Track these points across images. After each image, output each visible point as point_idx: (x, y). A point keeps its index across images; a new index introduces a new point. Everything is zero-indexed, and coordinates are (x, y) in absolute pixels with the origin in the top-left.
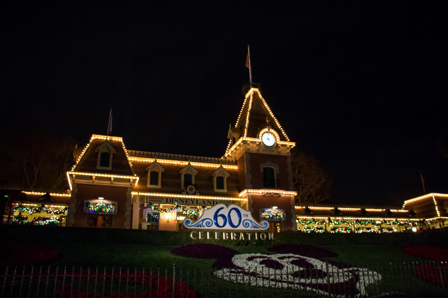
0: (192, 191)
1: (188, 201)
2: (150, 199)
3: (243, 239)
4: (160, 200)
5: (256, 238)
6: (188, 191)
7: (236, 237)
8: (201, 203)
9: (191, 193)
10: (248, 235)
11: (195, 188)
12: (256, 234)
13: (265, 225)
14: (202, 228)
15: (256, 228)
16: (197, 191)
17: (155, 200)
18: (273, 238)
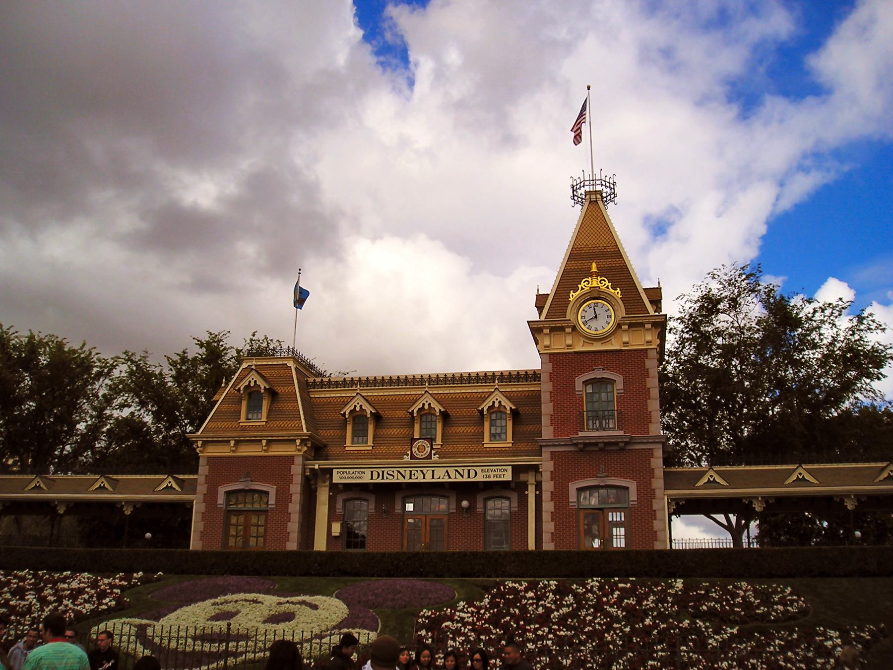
1: (414, 475)
8: (441, 477)
9: (422, 455)
11: (429, 445)
16: (433, 452)
17: (349, 475)
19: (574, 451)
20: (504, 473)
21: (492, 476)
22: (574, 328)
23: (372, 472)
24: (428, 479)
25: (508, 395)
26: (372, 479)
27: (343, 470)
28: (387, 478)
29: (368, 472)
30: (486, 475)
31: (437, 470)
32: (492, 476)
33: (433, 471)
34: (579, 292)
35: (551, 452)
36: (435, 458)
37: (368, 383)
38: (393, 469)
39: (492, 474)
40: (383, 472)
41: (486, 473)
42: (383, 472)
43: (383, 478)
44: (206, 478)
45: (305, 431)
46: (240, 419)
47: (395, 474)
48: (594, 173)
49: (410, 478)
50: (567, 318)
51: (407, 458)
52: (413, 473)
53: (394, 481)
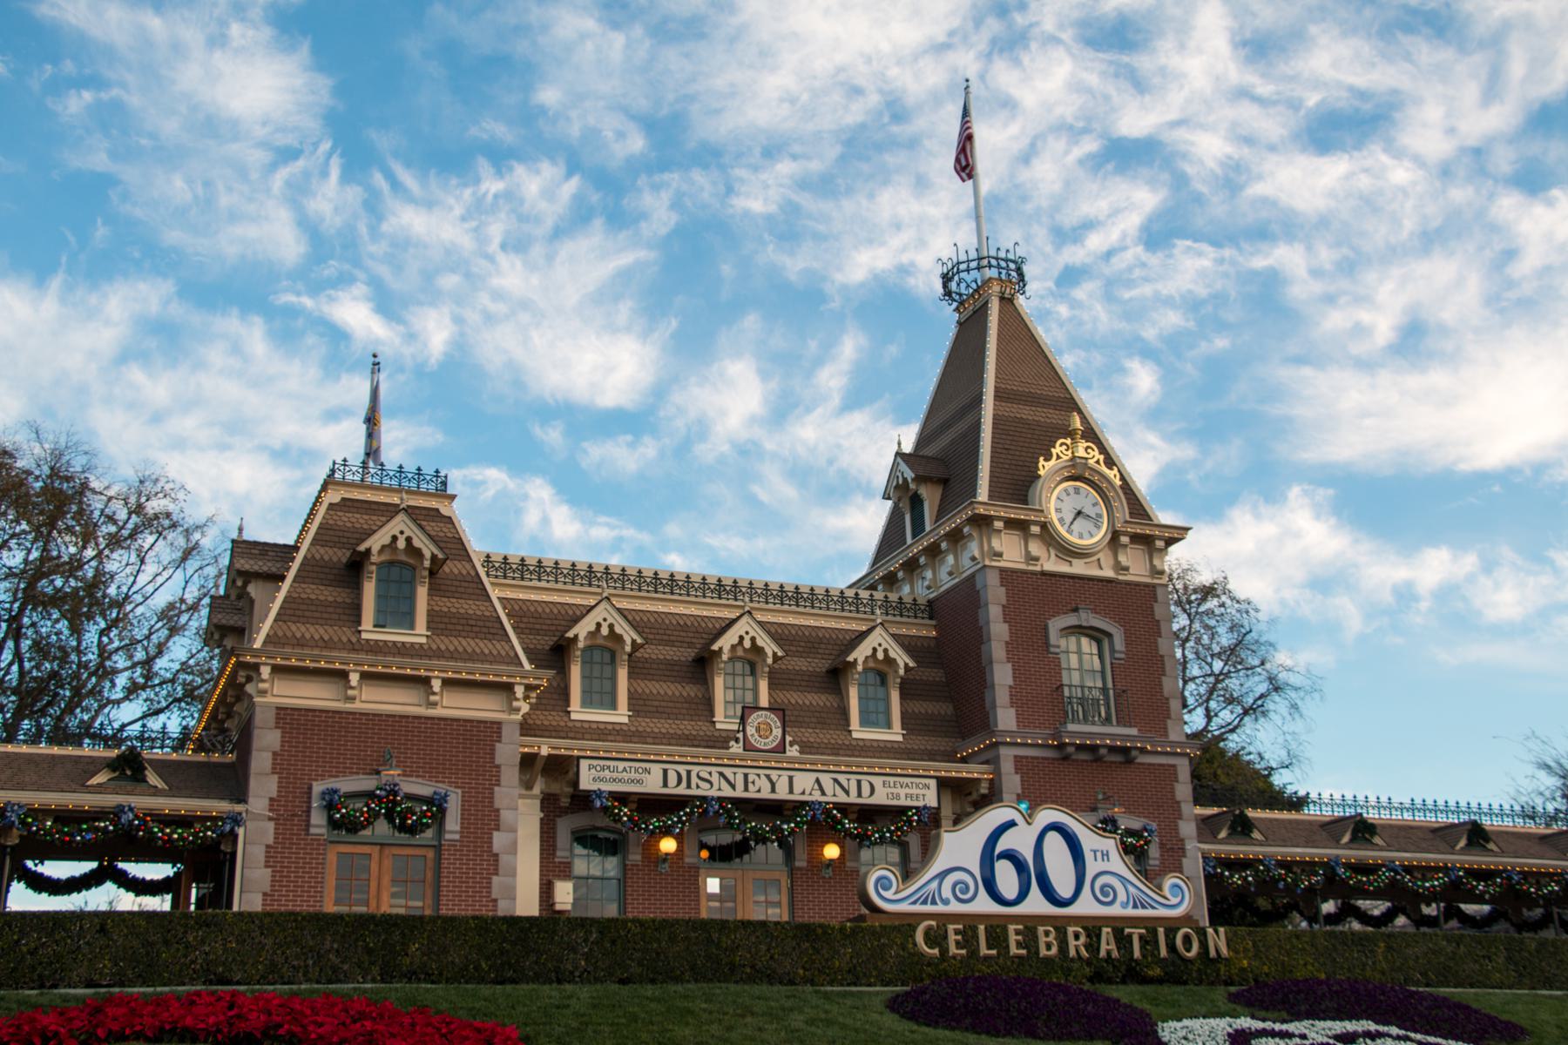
0: (767, 738)
1: (753, 783)
2: (593, 771)
3: (1115, 954)
4: (637, 776)
5: (1163, 952)
6: (752, 735)
7: (1087, 946)
8: (807, 792)
9: (765, 744)
10: (1130, 936)
11: (779, 724)
12: (1161, 930)
13: (1175, 896)
14: (940, 908)
15: (1144, 907)
16: (788, 738)
17: (615, 775)
18: (1224, 951)
19: (1053, 759)
20: (923, 791)
21: (903, 797)
22: (1044, 526)
23: (665, 772)
24: (782, 793)
25: (906, 643)
26: (665, 784)
27: (602, 763)
28: (698, 787)
29: (656, 770)
30: (893, 794)
31: (798, 776)
32: (903, 797)
33: (791, 778)
34: (1053, 462)
35: (1016, 757)
36: (793, 751)
37: (623, 579)
38: (709, 769)
39: (903, 792)
40: (689, 772)
41: (890, 790)
42: (689, 772)
43: (689, 786)
44: (274, 759)
45: (527, 666)
46: (359, 623)
47: (715, 778)
48: (985, 235)
49: (746, 789)
50: (1037, 507)
51: (736, 748)
52: (751, 778)
53: (714, 793)
